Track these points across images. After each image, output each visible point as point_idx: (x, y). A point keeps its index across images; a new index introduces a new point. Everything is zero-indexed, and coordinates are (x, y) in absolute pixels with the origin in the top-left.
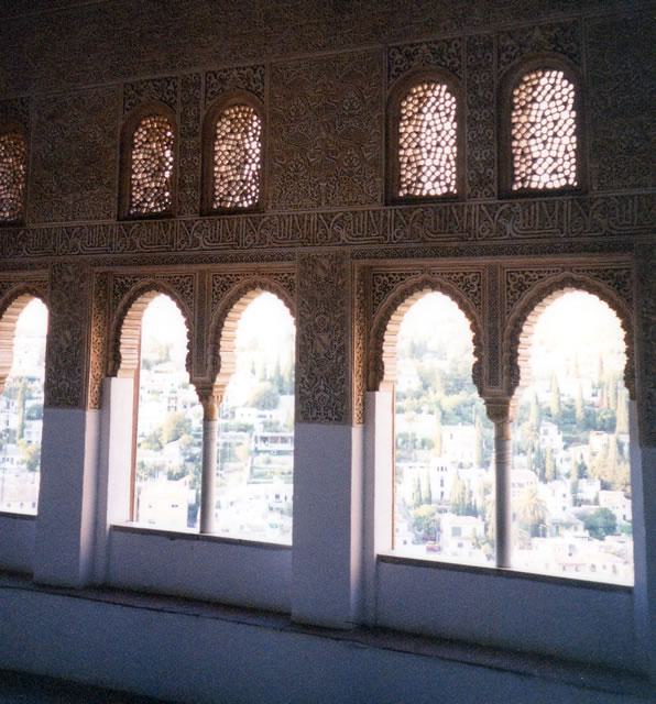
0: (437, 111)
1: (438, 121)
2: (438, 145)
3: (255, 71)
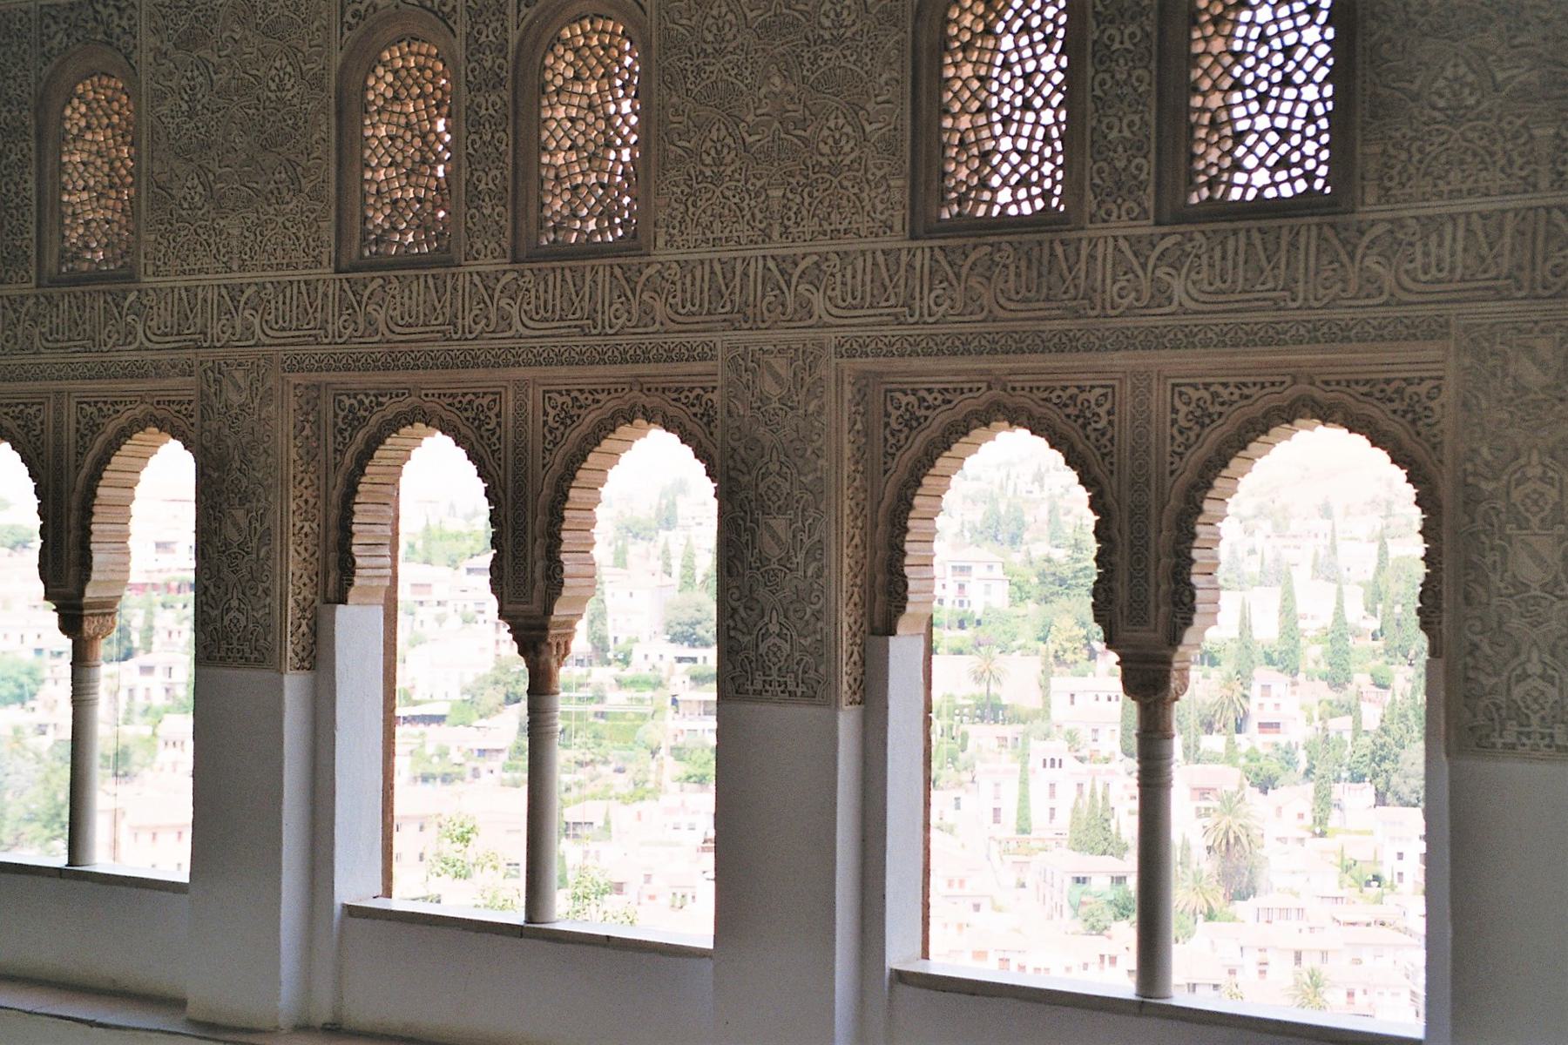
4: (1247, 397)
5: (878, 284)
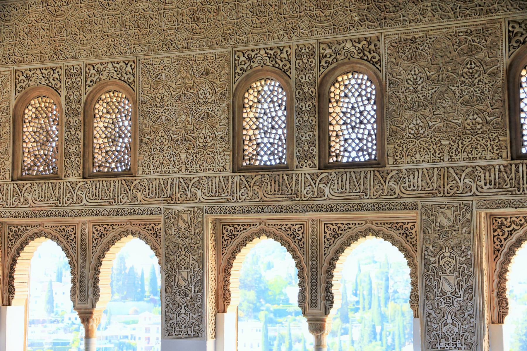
0: (360, 95)
1: (361, 104)
2: (361, 122)
3: (282, 51)
4: (246, 229)
5: (49, 193)
